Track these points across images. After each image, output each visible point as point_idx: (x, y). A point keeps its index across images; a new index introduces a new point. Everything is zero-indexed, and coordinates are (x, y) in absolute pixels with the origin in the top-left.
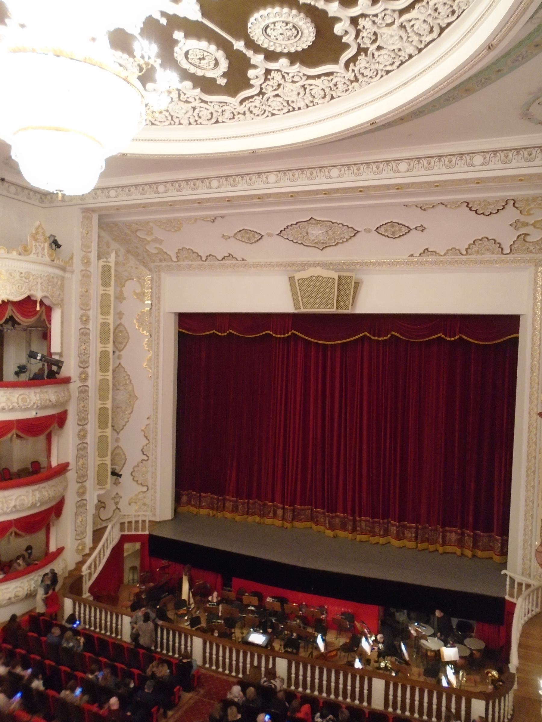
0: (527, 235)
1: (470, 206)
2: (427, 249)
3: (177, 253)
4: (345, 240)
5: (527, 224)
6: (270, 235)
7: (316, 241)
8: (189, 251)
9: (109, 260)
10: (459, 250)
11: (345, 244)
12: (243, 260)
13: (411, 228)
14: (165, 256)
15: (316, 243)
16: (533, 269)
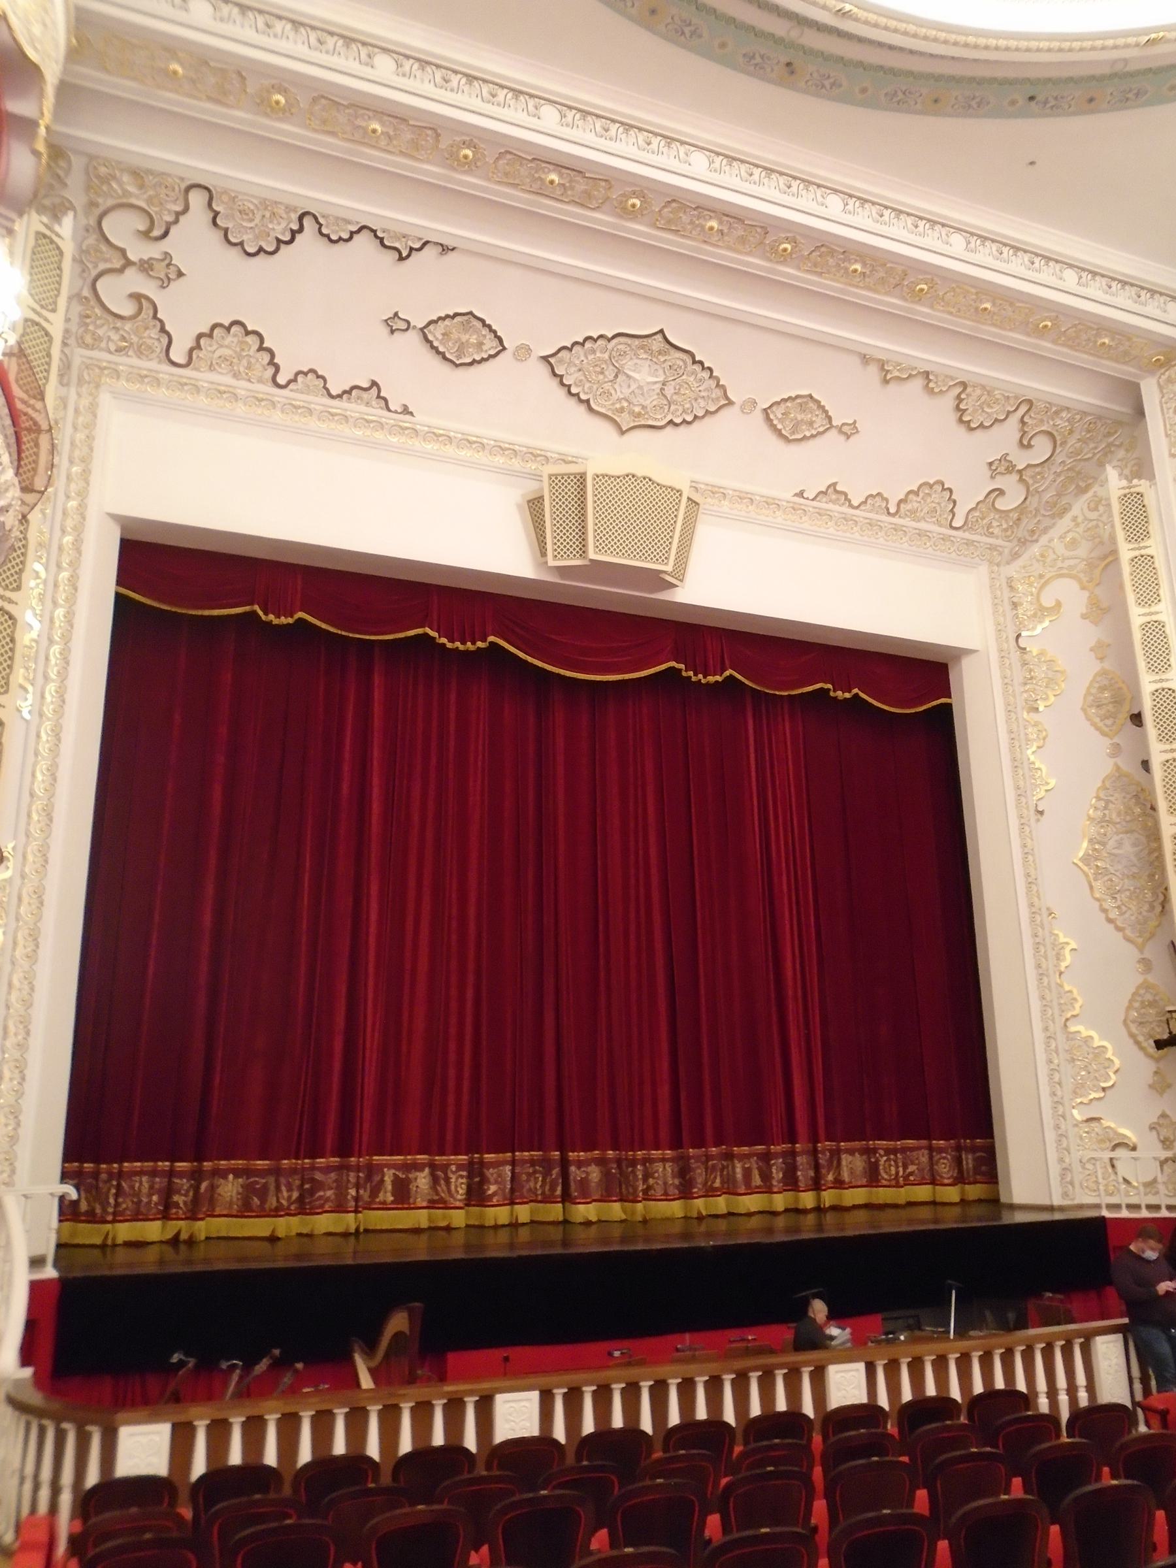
0: (1001, 492)
1: (963, 396)
2: (835, 484)
3: (200, 336)
4: (689, 418)
5: (1011, 468)
6: (524, 352)
7: (625, 404)
8: (252, 340)
9: (57, 228)
10: (887, 500)
11: (682, 428)
12: (406, 411)
13: (834, 423)
14: (154, 333)
15: (622, 410)
16: (984, 569)
